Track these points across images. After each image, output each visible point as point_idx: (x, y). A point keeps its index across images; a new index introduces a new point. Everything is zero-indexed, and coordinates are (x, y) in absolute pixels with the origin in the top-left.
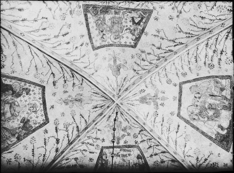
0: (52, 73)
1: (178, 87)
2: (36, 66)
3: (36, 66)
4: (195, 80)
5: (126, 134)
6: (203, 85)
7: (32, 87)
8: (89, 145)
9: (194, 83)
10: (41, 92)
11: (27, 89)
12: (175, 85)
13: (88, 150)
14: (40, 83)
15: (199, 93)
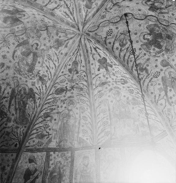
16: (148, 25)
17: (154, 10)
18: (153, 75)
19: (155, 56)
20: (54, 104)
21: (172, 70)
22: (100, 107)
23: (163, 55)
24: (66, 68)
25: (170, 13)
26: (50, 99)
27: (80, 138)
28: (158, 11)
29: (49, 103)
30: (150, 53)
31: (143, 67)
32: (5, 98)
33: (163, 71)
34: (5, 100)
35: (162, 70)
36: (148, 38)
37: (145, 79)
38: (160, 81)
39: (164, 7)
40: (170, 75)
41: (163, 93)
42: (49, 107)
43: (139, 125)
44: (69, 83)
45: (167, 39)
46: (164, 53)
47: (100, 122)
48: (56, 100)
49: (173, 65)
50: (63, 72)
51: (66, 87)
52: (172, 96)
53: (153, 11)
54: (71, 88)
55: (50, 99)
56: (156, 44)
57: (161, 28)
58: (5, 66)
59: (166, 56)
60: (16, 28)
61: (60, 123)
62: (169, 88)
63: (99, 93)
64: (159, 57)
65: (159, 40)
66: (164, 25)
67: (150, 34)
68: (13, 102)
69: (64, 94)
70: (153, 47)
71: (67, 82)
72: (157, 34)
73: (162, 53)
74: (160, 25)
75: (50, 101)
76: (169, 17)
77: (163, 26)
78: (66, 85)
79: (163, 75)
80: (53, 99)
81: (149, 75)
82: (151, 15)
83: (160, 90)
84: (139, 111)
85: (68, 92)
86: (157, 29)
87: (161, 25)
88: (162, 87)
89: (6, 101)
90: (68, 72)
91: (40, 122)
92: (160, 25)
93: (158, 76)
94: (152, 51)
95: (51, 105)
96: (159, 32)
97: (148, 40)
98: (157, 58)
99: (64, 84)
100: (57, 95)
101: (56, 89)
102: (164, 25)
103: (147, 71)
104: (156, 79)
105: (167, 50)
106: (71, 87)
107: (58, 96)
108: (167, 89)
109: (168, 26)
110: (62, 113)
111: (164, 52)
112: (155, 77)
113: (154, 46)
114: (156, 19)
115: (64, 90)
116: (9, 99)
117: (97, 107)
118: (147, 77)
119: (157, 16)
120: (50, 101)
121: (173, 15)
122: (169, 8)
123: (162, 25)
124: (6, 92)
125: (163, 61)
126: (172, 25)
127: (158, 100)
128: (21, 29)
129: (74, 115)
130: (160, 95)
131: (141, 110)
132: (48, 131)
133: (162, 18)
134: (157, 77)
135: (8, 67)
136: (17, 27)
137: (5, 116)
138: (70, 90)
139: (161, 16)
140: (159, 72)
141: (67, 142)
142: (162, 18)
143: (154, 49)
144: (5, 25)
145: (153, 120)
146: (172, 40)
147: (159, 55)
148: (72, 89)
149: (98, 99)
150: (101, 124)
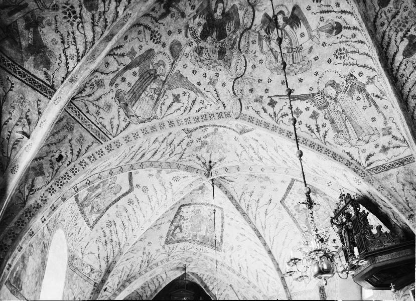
0: (266, 214)
1: (134, 184)
2: (276, 228)
3: (276, 228)
4: (118, 199)
5: (202, 139)
6: (110, 198)
7: (291, 208)
8: (256, 150)
9: (119, 195)
10: (287, 198)
11: (296, 210)
12: (138, 186)
13: (259, 144)
14: (283, 209)
15: (111, 188)
16: (238, 8)
17: (264, 25)
18: (156, 29)
19: (187, 27)
21: (168, 67)
23: (190, 44)
25: (263, 57)
28: (263, 33)
30: (195, 17)
31: (174, 6)
33: (162, 50)
35: (164, 45)
36: (218, 10)
37: (152, 17)
38: (146, 48)
39: (271, 46)
40: (158, 64)
41: (127, 60)
43: (27, 10)
45: (218, 50)
46: (194, 46)
49: (177, 68)
52: (128, 80)
53: (263, 22)
56: (208, 28)
57: (234, 37)
59: (188, 49)
62: (137, 69)
64: (186, 36)
65: (215, 34)
66: (240, 42)
67: (223, 13)
70: (203, 22)
72: (223, 29)
73: (192, 40)
74: (238, 33)
76: (255, 53)
77: (238, 39)
79: (156, 51)
81: (157, 22)
82: (254, 15)
83: (132, 52)
84: (68, 7)
86: (232, 29)
87: (239, 35)
88: (137, 55)
92: (238, 33)
93: (154, 40)
94: (197, 20)
96: (228, 33)
97: (215, 11)
98: (183, 32)
102: (240, 42)
103: (163, 16)
104: (148, 37)
105: (199, 51)
108: (136, 67)
109: (240, 50)
111: (195, 44)
112: (151, 35)
113: (205, 24)
114: (248, 27)
118: (154, 18)
119: (253, 27)
121: (261, 61)
122: (272, 55)
123: (240, 38)
125: (180, 44)
126: (243, 59)
127: (114, 54)
130: (123, 55)
131: (74, 12)
133: (251, 39)
134: (151, 39)
139: (254, 37)
140: (160, 42)
142: (251, 39)
143: (199, 24)
145: (64, 51)
146: (219, 59)
147: (189, 35)
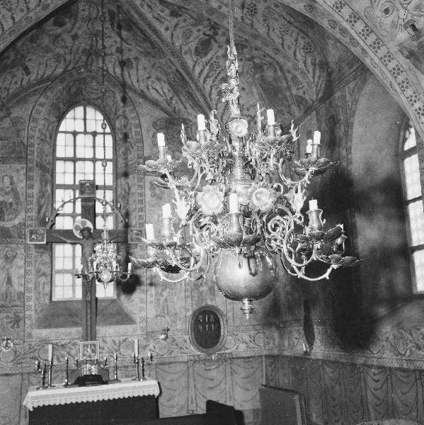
20: (218, 71)
22: (271, 29)
24: (162, 19)
26: (202, 71)
27: (295, 96)
29: (208, 76)
32: (171, 99)
34: (174, 102)
42: (214, 81)
44: (201, 27)
47: (297, 52)
48: (212, 64)
50: (167, 29)
51: (204, 34)
54: (213, 30)
55: (202, 71)
58: (133, 60)
60: (81, 14)
61: (255, 90)
63: (246, 10)
68: (183, 99)
69: (215, 45)
71: (194, 30)
75: (206, 72)
78: (201, 33)
80: (207, 67)
85: (217, 37)
89: (177, 102)
90: (176, 20)
91: (224, 110)
95: (215, 76)
99: (195, 34)
100: (206, 54)
101: (193, 52)
106: (210, 29)
107: (209, 56)
110: (245, 70)
115: (209, 40)
116: (176, 97)
117: (268, 33)
120: (206, 72)
124: (166, 91)
128: (87, 7)
129: (264, 62)
132: (248, 113)
135: (136, 59)
136: (80, 10)
137: (191, 123)
138: (216, 33)
141: (284, 115)
144: (69, 26)
148: (216, 30)
149: (254, 18)
150: (303, 54)
